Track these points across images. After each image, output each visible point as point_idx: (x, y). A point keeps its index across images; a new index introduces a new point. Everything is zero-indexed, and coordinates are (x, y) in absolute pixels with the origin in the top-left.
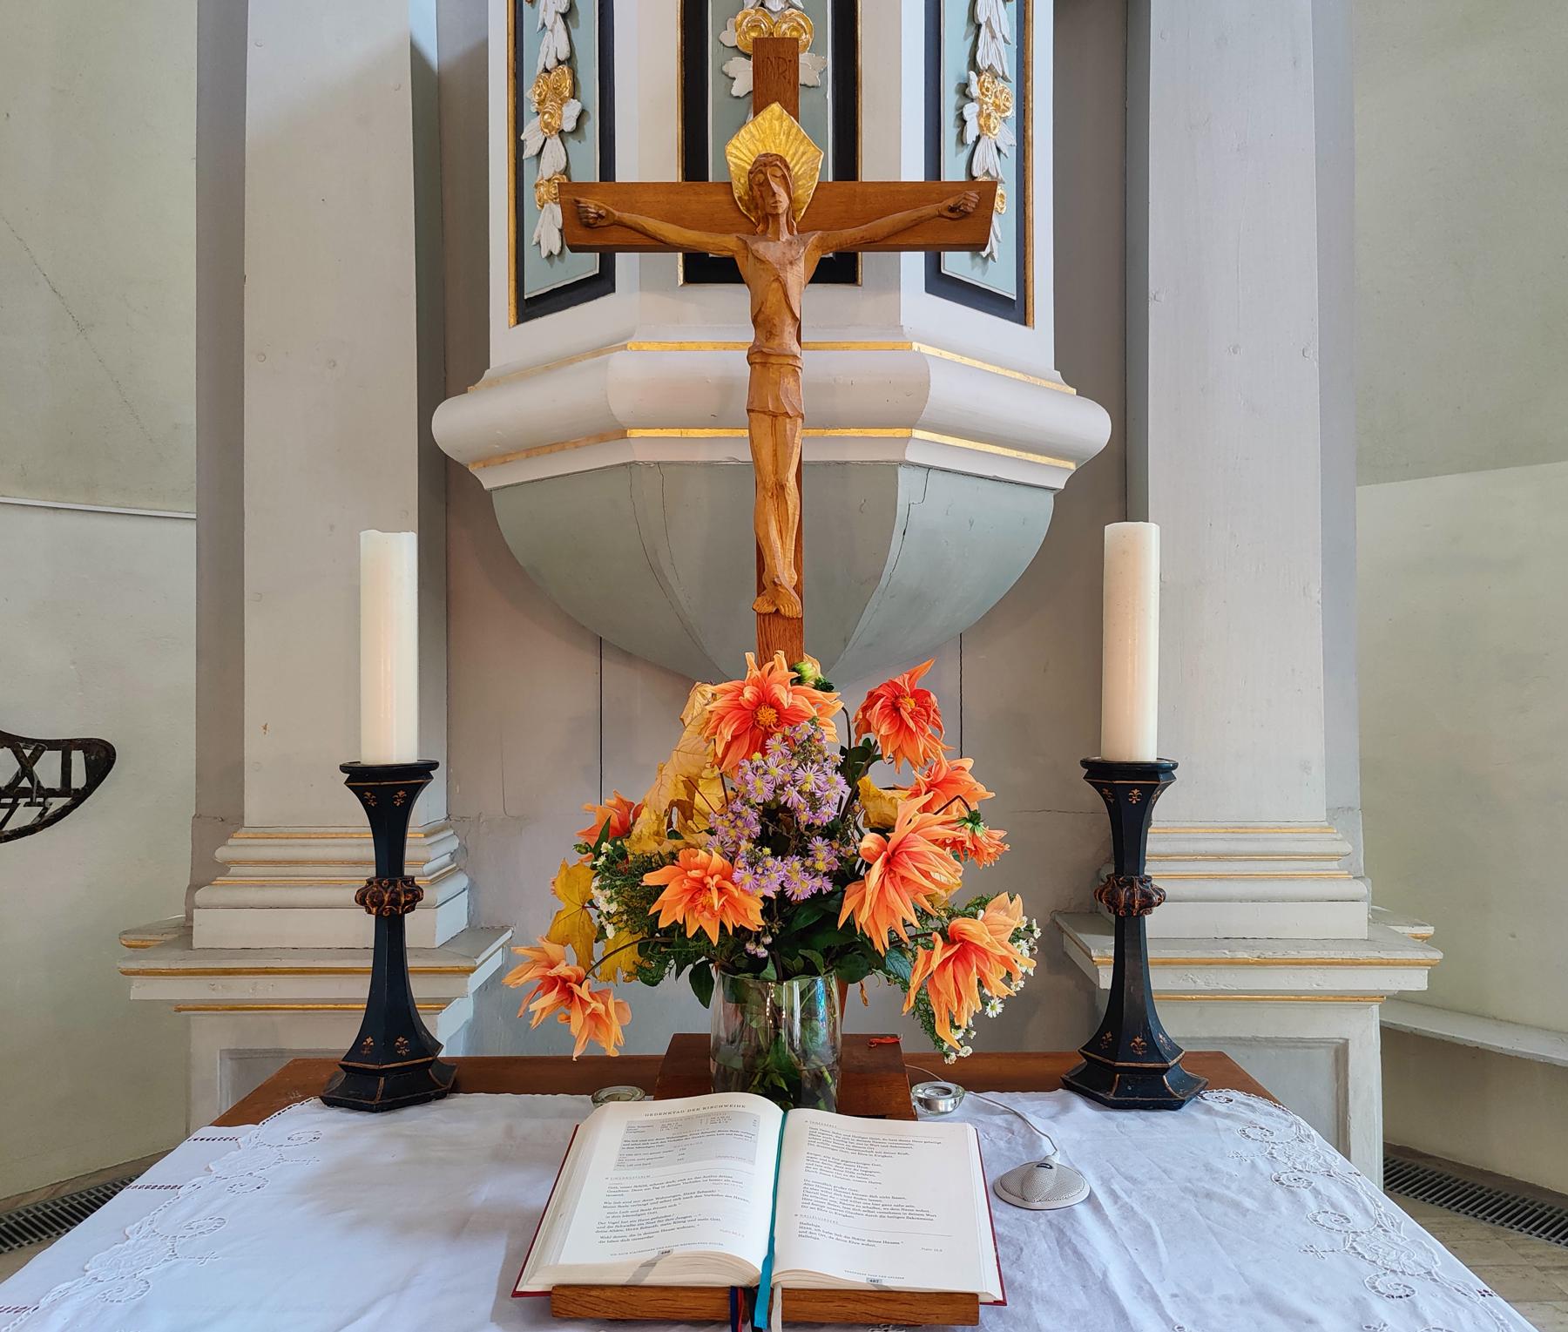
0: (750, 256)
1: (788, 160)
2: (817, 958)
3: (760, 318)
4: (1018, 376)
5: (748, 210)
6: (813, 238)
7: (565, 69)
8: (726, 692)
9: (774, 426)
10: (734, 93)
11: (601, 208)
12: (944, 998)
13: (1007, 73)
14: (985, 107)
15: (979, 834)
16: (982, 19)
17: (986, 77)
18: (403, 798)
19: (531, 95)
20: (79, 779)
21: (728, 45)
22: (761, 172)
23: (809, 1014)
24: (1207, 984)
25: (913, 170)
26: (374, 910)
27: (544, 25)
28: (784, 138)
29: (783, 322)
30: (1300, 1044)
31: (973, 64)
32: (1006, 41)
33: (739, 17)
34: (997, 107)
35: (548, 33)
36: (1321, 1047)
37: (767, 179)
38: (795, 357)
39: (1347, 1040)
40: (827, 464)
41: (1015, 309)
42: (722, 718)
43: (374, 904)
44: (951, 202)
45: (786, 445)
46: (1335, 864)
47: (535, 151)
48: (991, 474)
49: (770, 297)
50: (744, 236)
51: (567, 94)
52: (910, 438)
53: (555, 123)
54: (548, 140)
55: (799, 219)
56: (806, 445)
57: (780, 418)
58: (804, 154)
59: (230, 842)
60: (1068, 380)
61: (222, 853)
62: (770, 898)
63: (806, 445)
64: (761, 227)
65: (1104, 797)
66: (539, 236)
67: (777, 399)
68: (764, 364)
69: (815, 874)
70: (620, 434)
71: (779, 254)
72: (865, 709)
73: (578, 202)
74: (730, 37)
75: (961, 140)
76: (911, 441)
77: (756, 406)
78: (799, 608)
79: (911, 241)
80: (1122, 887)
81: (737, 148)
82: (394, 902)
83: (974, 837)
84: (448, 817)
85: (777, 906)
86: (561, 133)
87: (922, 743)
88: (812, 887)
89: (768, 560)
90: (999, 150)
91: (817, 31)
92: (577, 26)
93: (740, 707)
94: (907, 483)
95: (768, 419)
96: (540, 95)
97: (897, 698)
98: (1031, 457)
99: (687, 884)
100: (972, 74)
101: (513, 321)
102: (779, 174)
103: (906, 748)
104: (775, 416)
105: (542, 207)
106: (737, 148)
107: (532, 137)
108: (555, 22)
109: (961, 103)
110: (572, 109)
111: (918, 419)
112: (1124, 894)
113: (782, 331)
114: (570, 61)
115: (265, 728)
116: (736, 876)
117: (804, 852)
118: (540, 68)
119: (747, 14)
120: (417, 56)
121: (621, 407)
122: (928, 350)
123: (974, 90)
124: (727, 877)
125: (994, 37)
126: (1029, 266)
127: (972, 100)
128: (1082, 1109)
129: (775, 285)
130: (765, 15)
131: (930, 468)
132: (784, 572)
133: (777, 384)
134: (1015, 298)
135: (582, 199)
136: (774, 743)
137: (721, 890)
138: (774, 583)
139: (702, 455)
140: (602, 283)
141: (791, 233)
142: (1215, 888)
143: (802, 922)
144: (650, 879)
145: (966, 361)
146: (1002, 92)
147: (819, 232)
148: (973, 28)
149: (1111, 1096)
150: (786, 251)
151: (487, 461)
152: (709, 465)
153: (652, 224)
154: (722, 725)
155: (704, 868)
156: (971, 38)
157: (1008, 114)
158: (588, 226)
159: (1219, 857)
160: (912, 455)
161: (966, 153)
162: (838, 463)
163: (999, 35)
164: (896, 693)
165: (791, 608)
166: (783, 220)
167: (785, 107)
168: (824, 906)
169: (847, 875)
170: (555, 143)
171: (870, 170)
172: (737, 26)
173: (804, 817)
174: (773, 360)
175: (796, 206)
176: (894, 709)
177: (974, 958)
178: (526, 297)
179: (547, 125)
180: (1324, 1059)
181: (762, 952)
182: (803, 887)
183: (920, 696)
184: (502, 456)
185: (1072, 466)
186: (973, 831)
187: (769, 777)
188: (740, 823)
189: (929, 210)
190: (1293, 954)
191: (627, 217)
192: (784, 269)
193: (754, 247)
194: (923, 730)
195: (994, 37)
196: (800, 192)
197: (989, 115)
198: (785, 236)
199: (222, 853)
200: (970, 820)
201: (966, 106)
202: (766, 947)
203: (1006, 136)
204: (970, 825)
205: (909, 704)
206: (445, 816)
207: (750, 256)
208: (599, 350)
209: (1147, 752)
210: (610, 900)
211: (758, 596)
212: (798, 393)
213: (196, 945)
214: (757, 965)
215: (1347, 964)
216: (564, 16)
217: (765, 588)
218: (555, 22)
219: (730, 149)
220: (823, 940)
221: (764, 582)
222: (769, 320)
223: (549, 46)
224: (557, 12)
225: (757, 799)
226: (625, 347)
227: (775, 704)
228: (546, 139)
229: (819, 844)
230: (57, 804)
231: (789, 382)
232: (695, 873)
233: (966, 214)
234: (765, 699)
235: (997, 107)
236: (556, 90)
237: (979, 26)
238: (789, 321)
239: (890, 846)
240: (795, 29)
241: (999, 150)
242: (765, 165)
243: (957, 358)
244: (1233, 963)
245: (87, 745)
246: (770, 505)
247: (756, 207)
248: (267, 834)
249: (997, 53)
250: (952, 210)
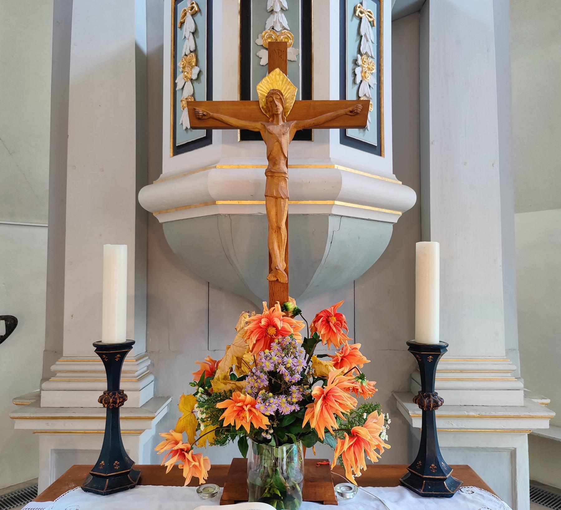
0: (266, 131)
1: (282, 91)
2: (293, 437)
3: (271, 157)
4: (378, 177)
5: (266, 112)
6: (293, 123)
7: (193, 55)
8: (254, 320)
9: (276, 202)
10: (261, 64)
11: (204, 111)
12: (349, 462)
13: (373, 55)
14: (364, 69)
15: (364, 384)
16: (363, 33)
17: (364, 57)
18: (119, 358)
19: (180, 64)
21: (259, 45)
22: (271, 97)
23: (290, 459)
24: (457, 425)
25: (334, 95)
26: (106, 406)
27: (185, 37)
28: (280, 82)
29: (280, 159)
30: (496, 450)
31: (359, 52)
32: (372, 42)
33: (263, 34)
34: (369, 69)
35: (187, 40)
36: (505, 451)
37: (273, 100)
38: (285, 173)
39: (515, 449)
40: (299, 215)
41: (377, 150)
42: (252, 332)
43: (106, 403)
44: (351, 109)
45: (281, 210)
46: (509, 375)
47: (181, 87)
48: (367, 218)
49: (275, 148)
50: (264, 123)
51: (194, 64)
52: (334, 204)
53: (189, 76)
54: (186, 83)
55: (287, 116)
57: (279, 199)
58: (289, 89)
59: (57, 363)
60: (399, 178)
61: (53, 368)
62: (271, 415)
64: (271, 119)
65: (417, 358)
66: (182, 121)
67: (277, 191)
68: (272, 176)
69: (291, 404)
70: (213, 203)
71: (278, 130)
72: (315, 322)
73: (195, 109)
74: (260, 42)
75: (354, 82)
76: (334, 206)
77: (269, 194)
78: (287, 279)
79: (334, 125)
80: (425, 398)
81: (261, 87)
82: (114, 402)
83: (362, 386)
84: (146, 351)
86: (191, 80)
87: (339, 337)
88: (291, 409)
89: (273, 259)
90: (370, 86)
91: (296, 39)
92: (198, 37)
93: (260, 327)
94: (332, 223)
95: (274, 200)
96: (183, 65)
97: (328, 317)
98: (384, 210)
99: (235, 409)
100: (359, 56)
101: (172, 155)
102: (279, 97)
103: (332, 339)
104: (276, 198)
105: (183, 109)
106: (261, 87)
107: (180, 81)
108: (189, 36)
109: (354, 67)
110: (196, 70)
111: (337, 197)
112: (426, 401)
113: (280, 163)
114: (195, 51)
115: (72, 316)
116: (257, 406)
117: (287, 393)
118: (183, 54)
119: (267, 32)
120: (138, 49)
121: (213, 192)
122: (341, 168)
123: (360, 62)
124: (253, 406)
125: (367, 41)
126: (382, 132)
127: (359, 66)
128: (409, 497)
129: (277, 143)
130: (274, 32)
131: (342, 216)
132: (281, 264)
133: (277, 185)
134: (376, 145)
135: (197, 108)
136: (274, 345)
137: (250, 410)
138: (276, 269)
139: (247, 211)
140: (207, 141)
141: (284, 121)
142: (460, 384)
143: (286, 423)
144: (219, 405)
145: (357, 172)
146: (371, 63)
147: (295, 121)
148: (359, 37)
149: (422, 492)
150: (282, 129)
151: (160, 212)
152: (250, 215)
153: (226, 118)
154: (252, 335)
155: (243, 401)
156: (358, 41)
157: (373, 71)
158: (199, 119)
159: (462, 371)
160: (334, 212)
161: (356, 87)
162: (303, 215)
163: (370, 40)
164: (328, 316)
165: (283, 279)
166: (280, 116)
167: (281, 69)
168: (297, 417)
170: (189, 84)
171: (317, 95)
172: (263, 37)
173: (287, 379)
174: (276, 175)
175: (285, 110)
176: (327, 322)
177: (363, 443)
178: (177, 145)
179: (186, 77)
180: (506, 456)
181: (269, 437)
182: (287, 410)
183: (338, 316)
184: (166, 210)
185: (400, 213)
186: (362, 383)
187: (272, 361)
188: (259, 381)
189: (342, 112)
190: (493, 413)
191: (216, 115)
192: (280, 135)
193: (268, 127)
194: (339, 331)
195: (367, 41)
196: (287, 104)
197: (366, 72)
198: (281, 123)
199: (53, 368)
200: (360, 378)
201: (356, 68)
202: (271, 434)
203: (372, 80)
204: (360, 380)
205: (333, 320)
206: (145, 351)
207: (266, 131)
208: (205, 168)
209: (434, 339)
210: (202, 413)
211: (270, 273)
212: (285, 188)
213: (42, 406)
214: (267, 441)
215: (516, 418)
216: (193, 33)
217: (272, 270)
218: (189, 36)
219: (258, 87)
220: (296, 430)
221: (272, 268)
222: (274, 158)
223: (187, 45)
224: (190, 32)
225: (266, 369)
226: (215, 167)
227: (275, 326)
228: (185, 82)
229: (294, 389)
231: (283, 184)
232: (239, 404)
233: (357, 114)
234: (271, 323)
235: (369, 69)
236: (190, 63)
237: (361, 37)
238: (282, 158)
239: (325, 393)
240: (286, 38)
241: (370, 86)
242: (273, 94)
243: (353, 171)
244: (468, 417)
246: (274, 236)
247: (269, 111)
248: (73, 360)
249: (369, 47)
250: (351, 112)
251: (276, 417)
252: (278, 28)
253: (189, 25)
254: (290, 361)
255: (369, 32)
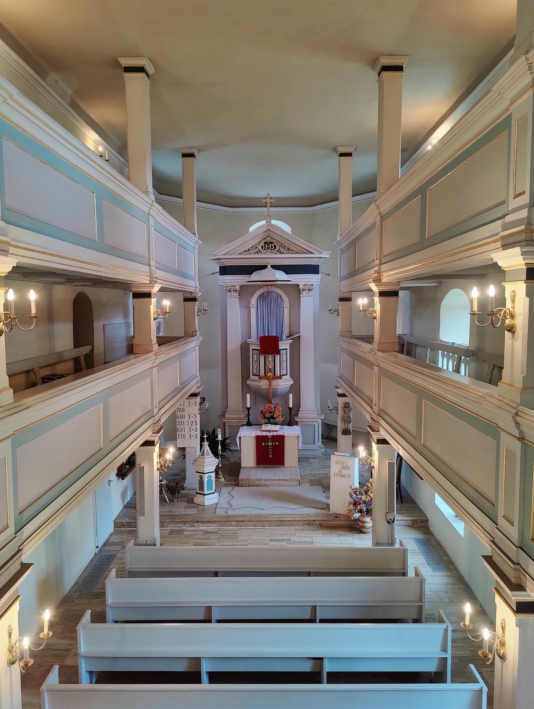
20: (202, 402)
41: (287, 375)
56: (272, 387)
63: (272, 387)
85: (271, 416)
128: (287, 426)
168: (273, 416)
169: (274, 414)
180: (314, 426)
182: (272, 415)
184: (251, 385)
203: (285, 364)
209: (291, 407)
221: (270, 398)
223: (255, 359)
230: (201, 404)
234: (270, 406)
245: (203, 398)
249: (285, 359)
251: (271, 416)
252: (270, 361)
253: (255, 356)
254: (272, 410)
255: (285, 356)
